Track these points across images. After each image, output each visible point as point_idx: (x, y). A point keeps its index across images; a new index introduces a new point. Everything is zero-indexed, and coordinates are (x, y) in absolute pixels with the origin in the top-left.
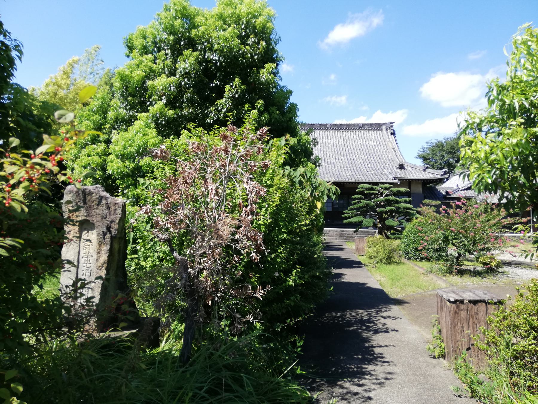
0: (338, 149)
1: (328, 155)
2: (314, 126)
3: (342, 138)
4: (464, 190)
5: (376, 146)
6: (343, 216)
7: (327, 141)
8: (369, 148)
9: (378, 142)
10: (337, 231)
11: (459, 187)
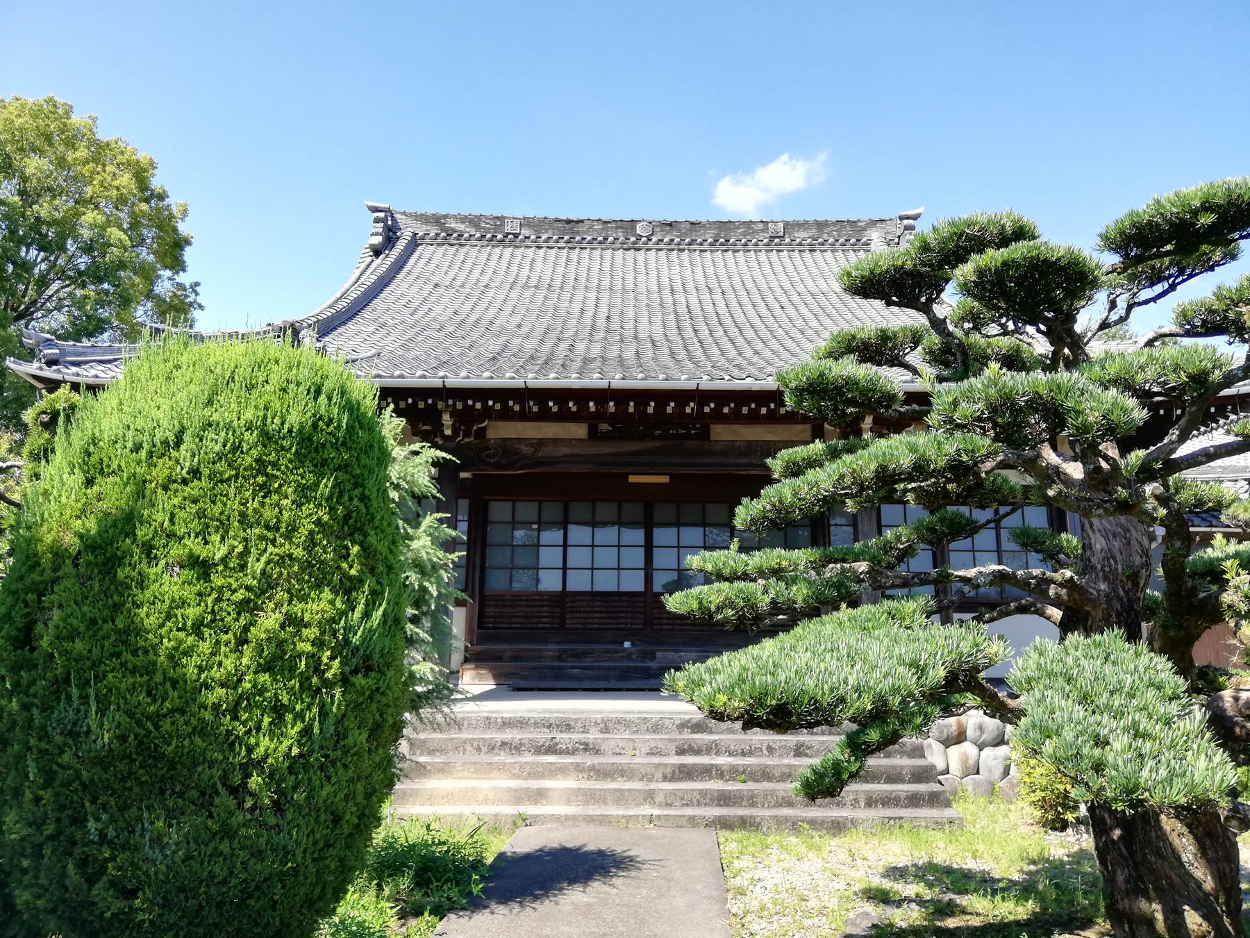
2: (580, 228)
3: (699, 270)
8: (821, 299)
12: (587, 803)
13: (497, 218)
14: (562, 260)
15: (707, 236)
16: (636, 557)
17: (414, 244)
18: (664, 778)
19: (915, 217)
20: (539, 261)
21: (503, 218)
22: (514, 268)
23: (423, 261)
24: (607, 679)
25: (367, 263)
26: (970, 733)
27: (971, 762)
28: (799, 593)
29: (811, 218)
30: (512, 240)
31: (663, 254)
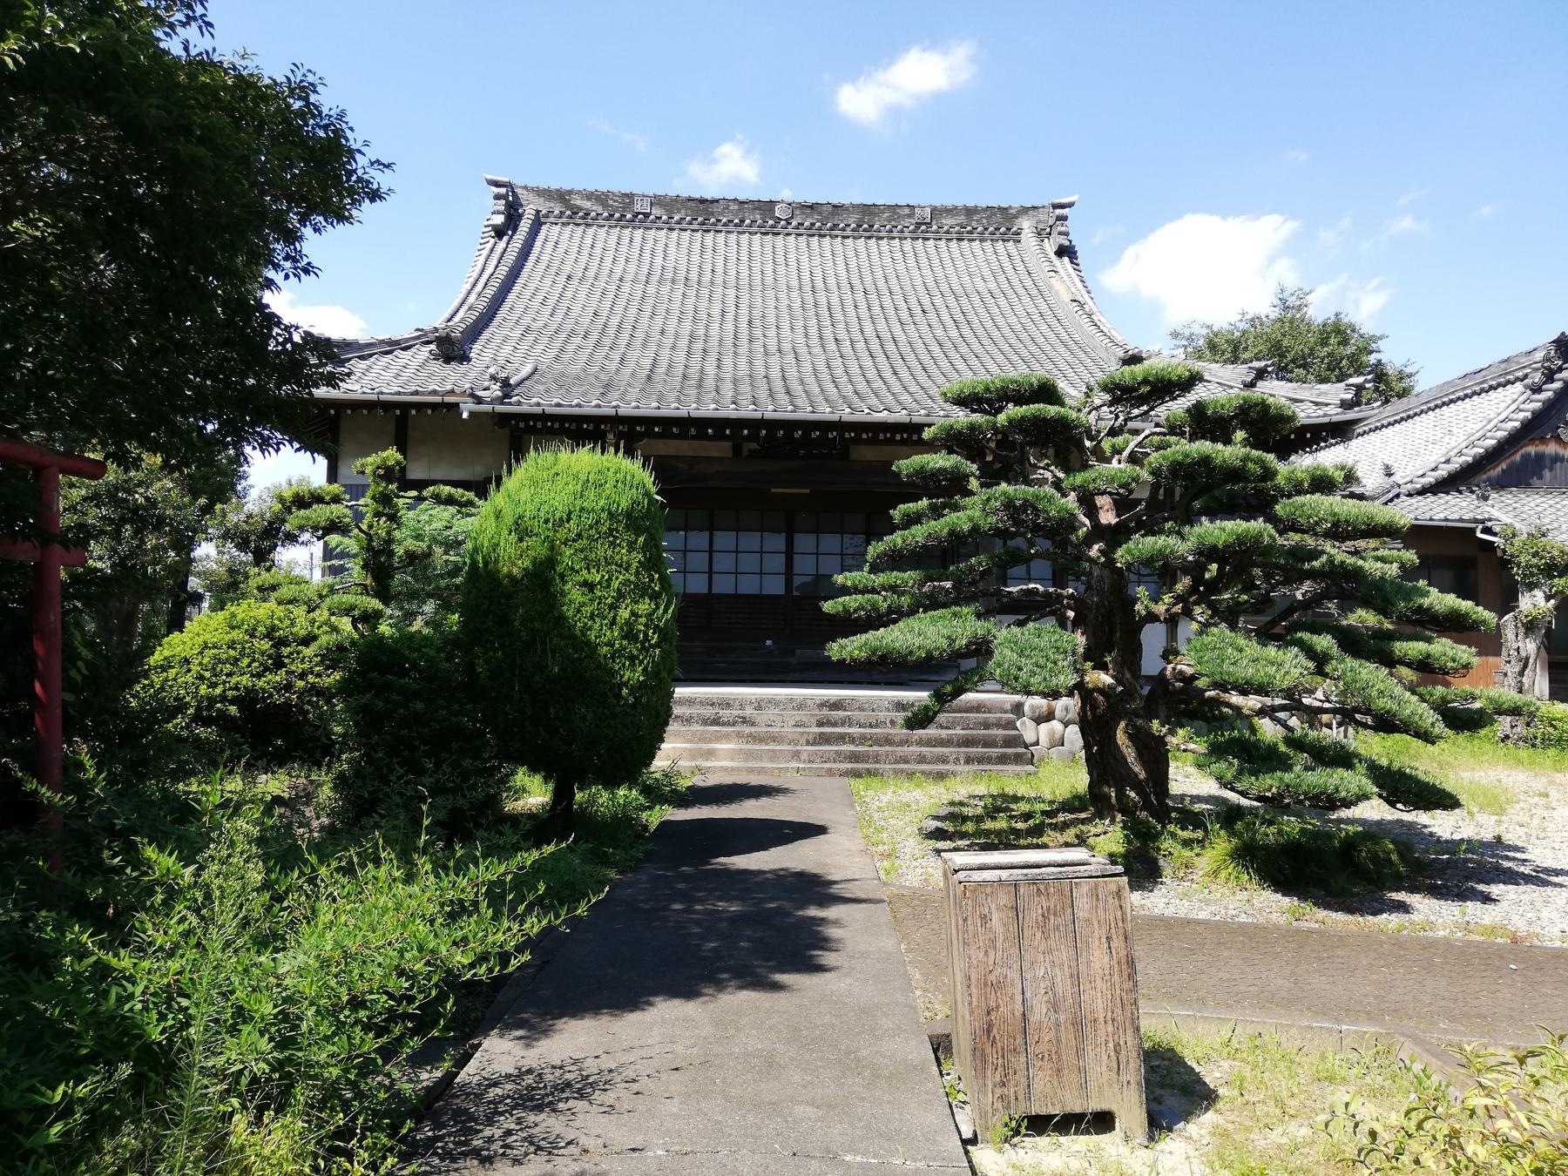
0: (823, 301)
1: (771, 319)
2: (716, 209)
3: (840, 261)
4: (1422, 492)
5: (997, 293)
6: (828, 606)
7: (769, 268)
8: (964, 301)
9: (1002, 279)
10: (801, 706)
11: (1397, 478)
12: (747, 760)
14: (697, 246)
15: (851, 221)
16: (778, 563)
18: (808, 743)
19: (1070, 205)
20: (672, 245)
21: (631, 196)
22: (647, 255)
23: (550, 245)
25: (489, 246)
26: (1057, 713)
27: (1057, 736)
28: (905, 601)
29: (960, 203)
30: (642, 220)
31: (802, 239)
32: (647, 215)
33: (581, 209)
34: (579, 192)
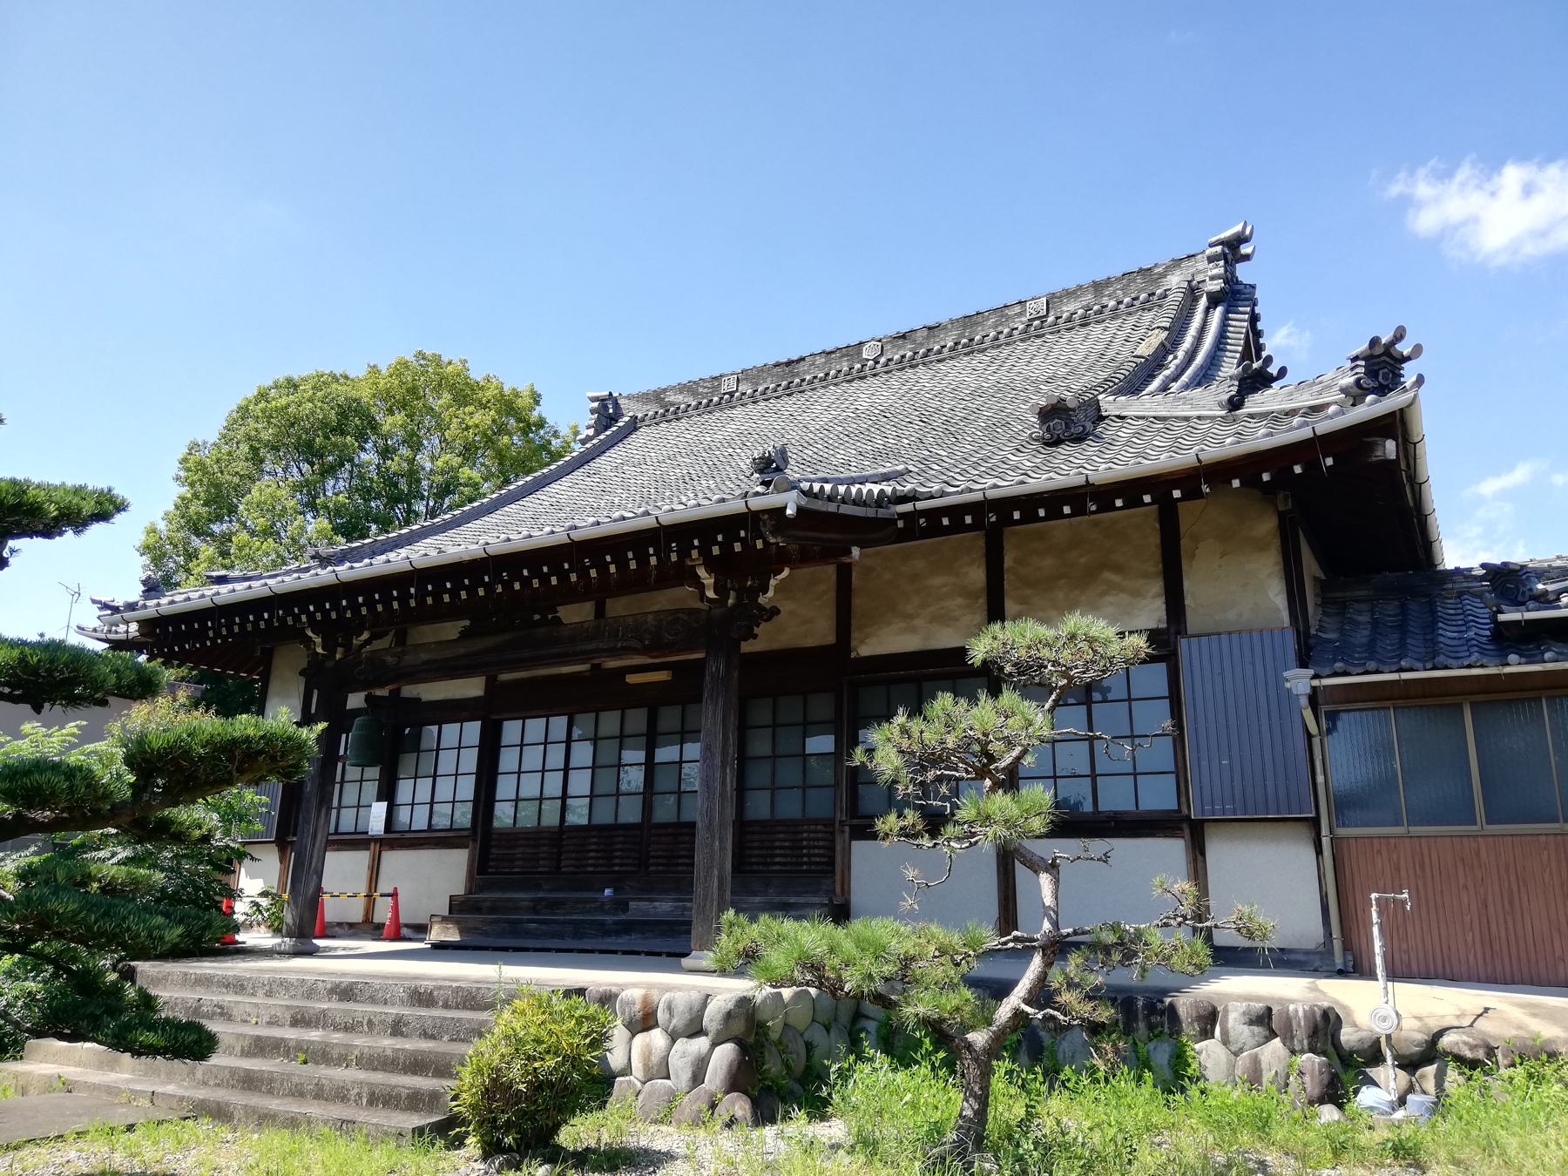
2: (802, 367)
13: (715, 378)
17: (633, 426)
24: (561, 936)
26: (661, 1016)
27: (655, 1059)
29: (1086, 280)
30: (730, 400)
32: (731, 394)
33: (672, 404)
34: (672, 388)
